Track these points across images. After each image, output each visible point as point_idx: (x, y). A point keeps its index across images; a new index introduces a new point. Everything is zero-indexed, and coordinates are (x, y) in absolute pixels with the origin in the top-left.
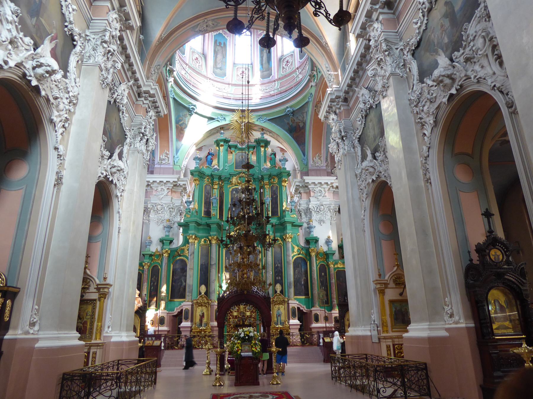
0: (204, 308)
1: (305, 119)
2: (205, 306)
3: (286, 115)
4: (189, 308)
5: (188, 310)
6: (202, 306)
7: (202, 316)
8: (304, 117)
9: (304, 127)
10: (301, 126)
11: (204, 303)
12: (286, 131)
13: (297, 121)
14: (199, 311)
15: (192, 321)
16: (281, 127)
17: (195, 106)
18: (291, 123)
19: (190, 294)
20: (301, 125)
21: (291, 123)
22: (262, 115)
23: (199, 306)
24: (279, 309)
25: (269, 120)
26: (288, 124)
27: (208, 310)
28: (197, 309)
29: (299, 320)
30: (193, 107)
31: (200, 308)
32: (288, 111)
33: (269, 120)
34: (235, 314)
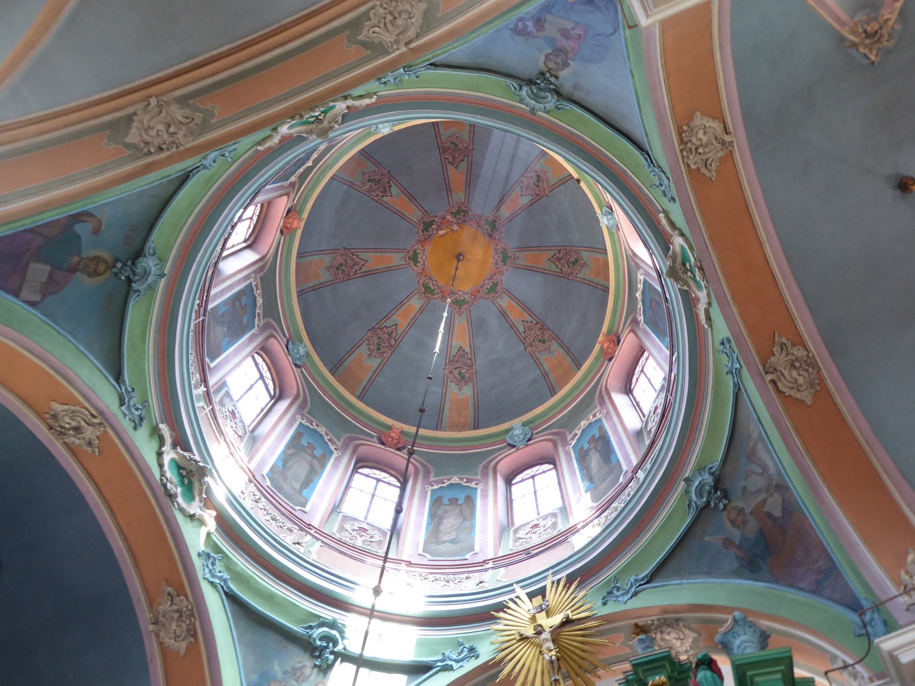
1: (772, 469)
3: (702, 513)
8: (764, 468)
9: (790, 508)
10: (777, 513)
12: (737, 574)
13: (749, 506)
16: (709, 573)
17: (333, 625)
18: (736, 535)
20: (774, 506)
21: (736, 535)
22: (616, 578)
25: (650, 579)
26: (728, 543)
30: (326, 629)
32: (699, 492)
33: (650, 579)
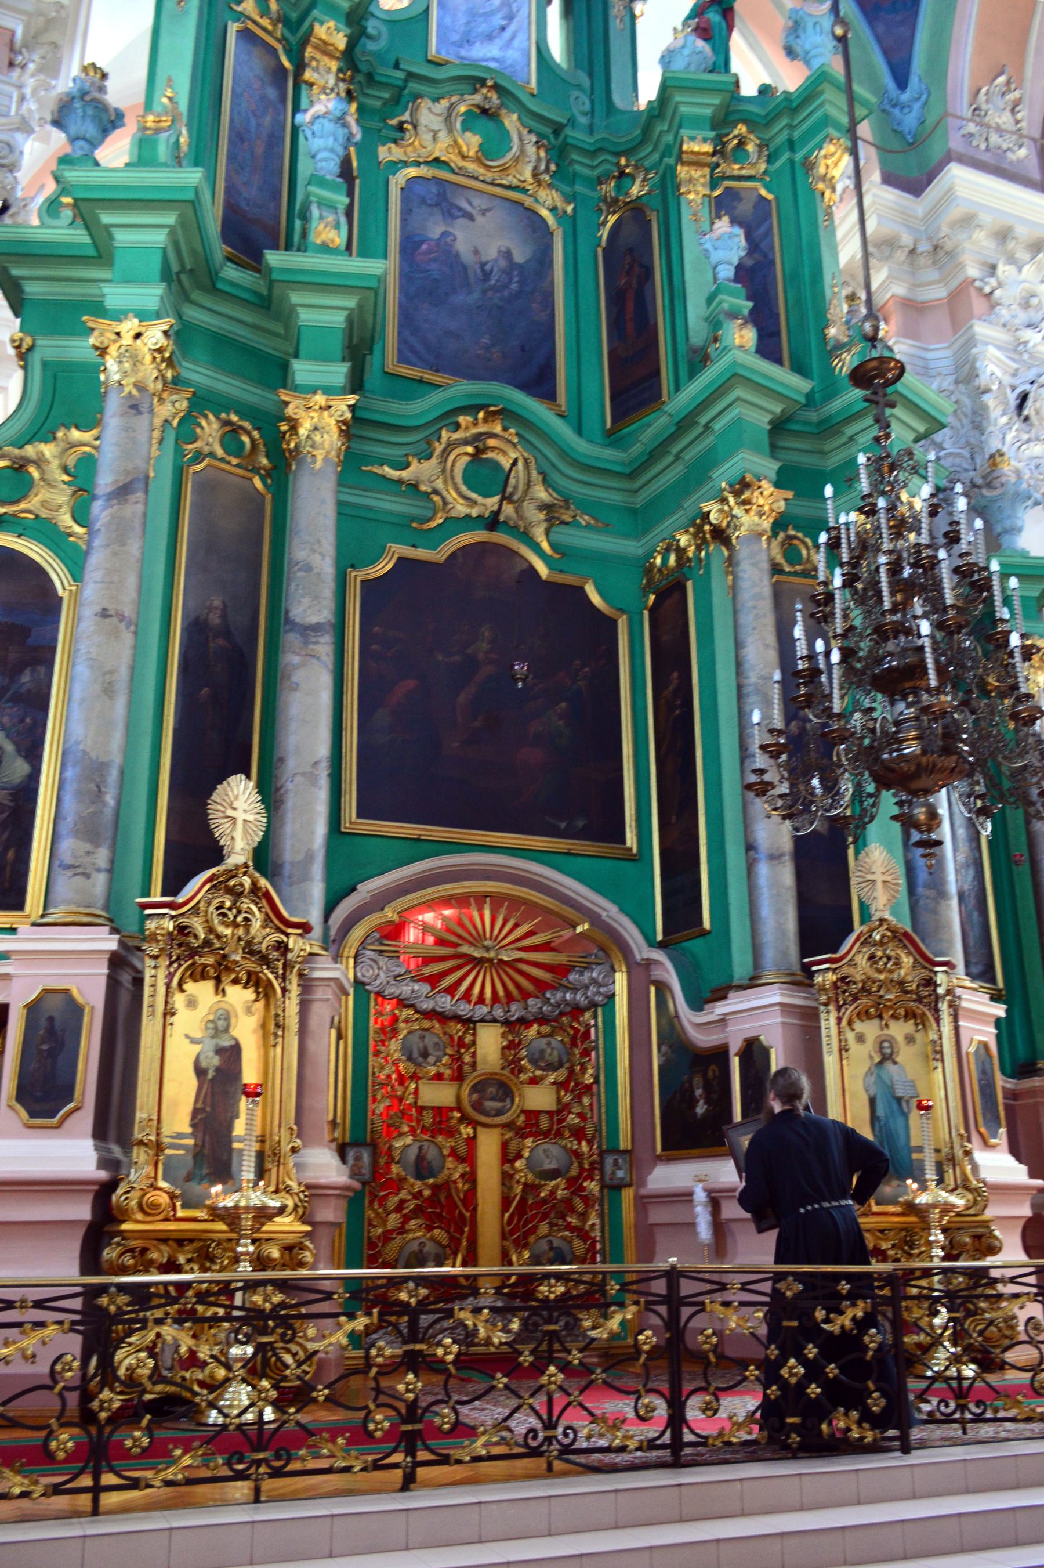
0: (238, 996)
2: (253, 981)
4: (90, 988)
5: (75, 1010)
6: (220, 973)
7: (221, 1081)
11: (250, 949)
14: (185, 1027)
15: (113, 1123)
19: (102, 856)
23: (199, 974)
24: (886, 1056)
27: (272, 1028)
28: (179, 1000)
29: (1015, 1151)
31: (202, 991)
34: (438, 1094)
